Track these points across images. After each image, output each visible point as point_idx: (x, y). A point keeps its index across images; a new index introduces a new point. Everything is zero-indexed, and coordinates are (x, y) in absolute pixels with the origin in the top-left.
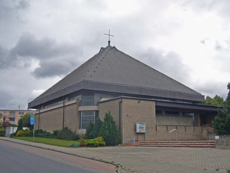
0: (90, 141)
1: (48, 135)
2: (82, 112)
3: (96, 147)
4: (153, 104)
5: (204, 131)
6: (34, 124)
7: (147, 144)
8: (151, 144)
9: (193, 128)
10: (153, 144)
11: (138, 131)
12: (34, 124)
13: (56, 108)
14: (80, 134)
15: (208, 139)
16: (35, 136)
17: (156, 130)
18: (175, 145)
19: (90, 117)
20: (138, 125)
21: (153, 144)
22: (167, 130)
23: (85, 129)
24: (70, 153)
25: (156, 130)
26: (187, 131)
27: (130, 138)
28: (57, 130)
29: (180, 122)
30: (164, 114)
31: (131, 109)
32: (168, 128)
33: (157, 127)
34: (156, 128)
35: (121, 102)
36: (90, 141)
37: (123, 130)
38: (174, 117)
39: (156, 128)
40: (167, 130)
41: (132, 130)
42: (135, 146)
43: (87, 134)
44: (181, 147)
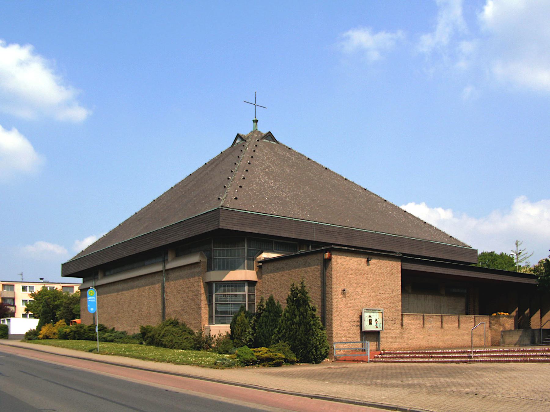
0: (261, 353)
1: (122, 338)
2: (214, 285)
3: (278, 365)
4: (396, 267)
5: (493, 327)
6: (95, 313)
7: (402, 358)
8: (415, 357)
9: (473, 320)
10: (422, 358)
11: (367, 327)
12: (95, 313)
13: (139, 275)
14: (215, 336)
15: (504, 343)
16: (99, 341)
17: (402, 325)
18: (486, 359)
19: (236, 295)
20: (366, 315)
21: (422, 358)
22: (423, 325)
23: (225, 323)
24: (387, 403)
25: (402, 325)
26: (462, 326)
27: (348, 344)
28: (147, 326)
29: (441, 307)
30: (410, 291)
31: (351, 276)
32: (425, 322)
33: (404, 319)
34: (402, 320)
35: (330, 259)
36: (260, 351)
37: (334, 325)
38: (430, 297)
39: (402, 320)
40: (423, 325)
41: (352, 325)
42: (371, 361)
43: (232, 336)
44: (509, 361)
